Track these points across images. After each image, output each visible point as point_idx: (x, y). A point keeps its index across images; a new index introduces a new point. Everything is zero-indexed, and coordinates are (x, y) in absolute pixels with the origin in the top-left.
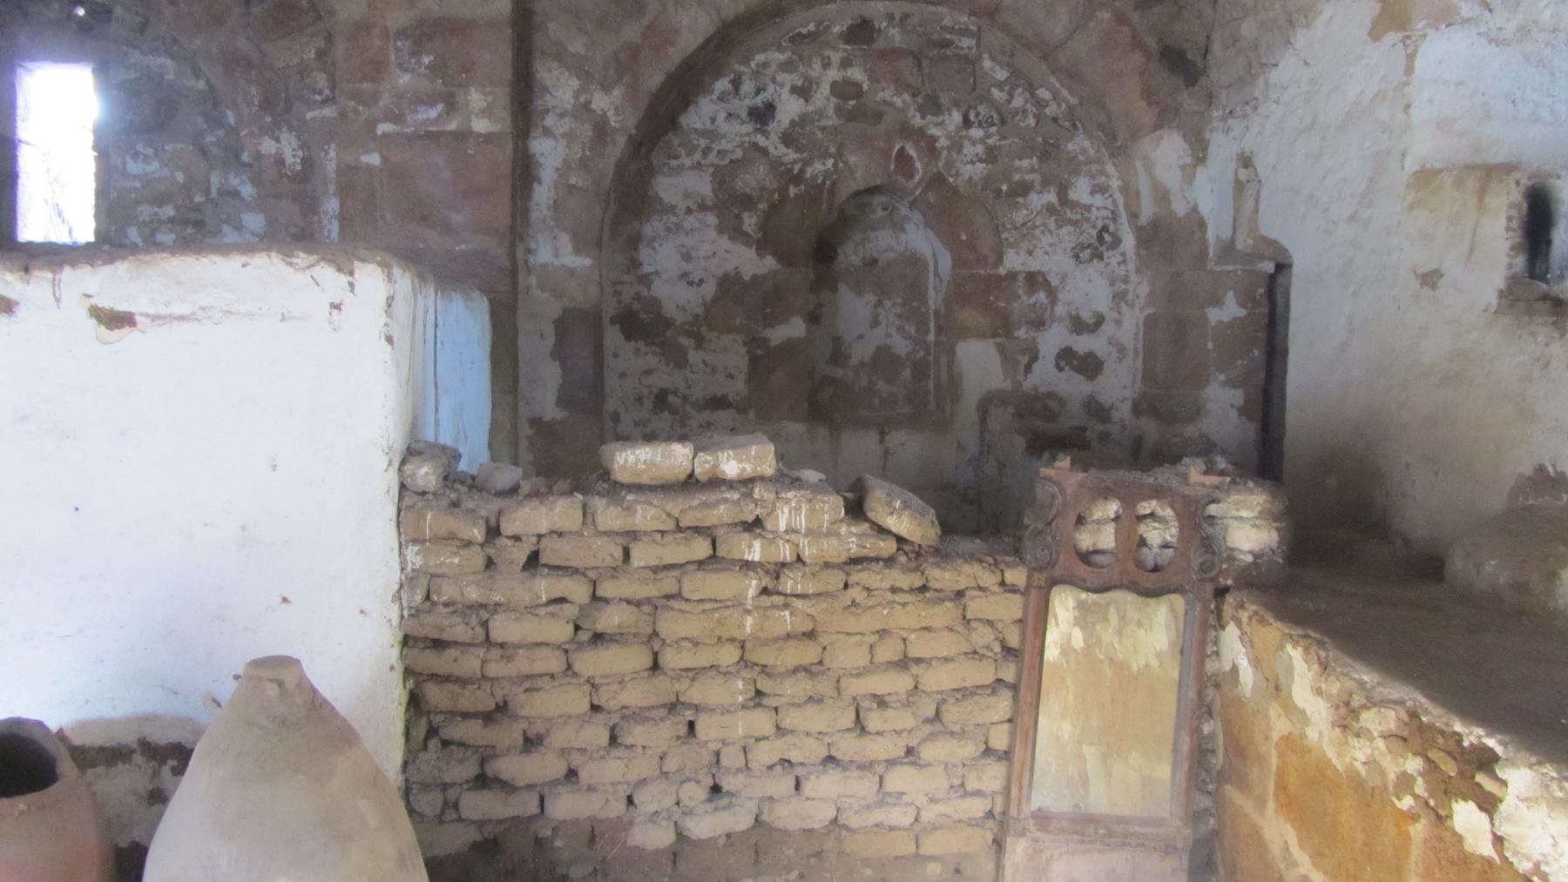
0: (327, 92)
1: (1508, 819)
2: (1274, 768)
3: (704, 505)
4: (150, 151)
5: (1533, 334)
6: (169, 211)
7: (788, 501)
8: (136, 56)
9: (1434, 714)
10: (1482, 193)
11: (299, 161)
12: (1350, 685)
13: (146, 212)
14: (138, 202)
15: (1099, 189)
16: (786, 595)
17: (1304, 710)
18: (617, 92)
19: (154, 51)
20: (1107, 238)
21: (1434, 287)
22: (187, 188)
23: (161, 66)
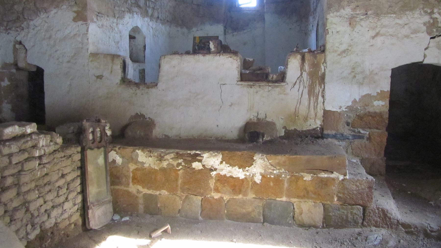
1: (205, 162)
2: (131, 176)
3: (24, 143)
7: (41, 138)
9: (181, 152)
10: (113, 60)
12: (159, 153)
16: (43, 164)
17: (143, 162)
21: (101, 79)
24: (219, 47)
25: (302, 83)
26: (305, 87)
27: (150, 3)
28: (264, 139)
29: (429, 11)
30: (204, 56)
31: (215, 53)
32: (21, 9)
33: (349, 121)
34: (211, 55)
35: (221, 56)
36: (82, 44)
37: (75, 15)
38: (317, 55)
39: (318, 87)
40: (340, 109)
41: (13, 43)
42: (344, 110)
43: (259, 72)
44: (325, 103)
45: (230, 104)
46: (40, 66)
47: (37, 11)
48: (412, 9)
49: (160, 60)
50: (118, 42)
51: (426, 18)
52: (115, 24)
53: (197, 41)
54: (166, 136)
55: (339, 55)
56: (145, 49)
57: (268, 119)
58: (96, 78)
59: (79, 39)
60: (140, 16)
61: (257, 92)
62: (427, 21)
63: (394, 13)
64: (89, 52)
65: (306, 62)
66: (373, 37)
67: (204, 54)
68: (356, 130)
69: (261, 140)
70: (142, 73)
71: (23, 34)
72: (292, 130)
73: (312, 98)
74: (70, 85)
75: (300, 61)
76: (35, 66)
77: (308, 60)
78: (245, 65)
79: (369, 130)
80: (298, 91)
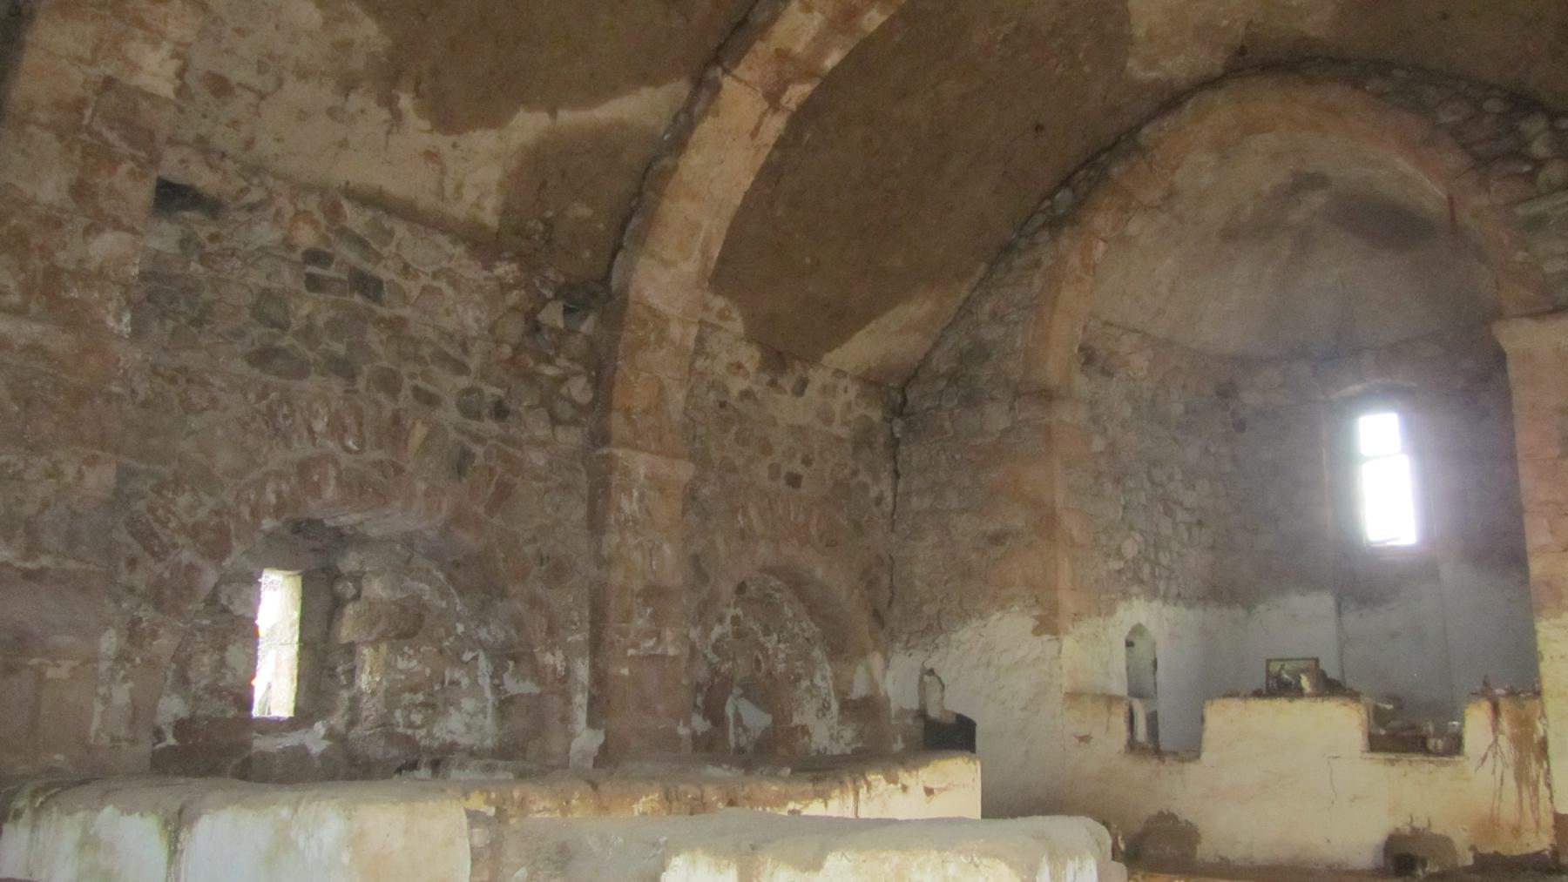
0: (578, 624)
4: (411, 652)
6: (420, 697)
8: (408, 582)
10: (1109, 708)
11: (563, 669)
13: (407, 697)
14: (402, 691)
18: (699, 628)
19: (420, 579)
20: (826, 705)
22: (430, 679)
23: (421, 590)
25: (1498, 757)
26: (1506, 765)
28: (1427, 869)
31: (1312, 696)
34: (1305, 699)
35: (1325, 702)
37: (1038, 623)
38: (1525, 703)
39: (1534, 766)
43: (1405, 734)
44: (1555, 800)
47: (964, 616)
49: (1202, 708)
50: (1107, 663)
52: (1100, 630)
54: (1222, 858)
57: (1436, 830)
58: (1077, 741)
60: (1142, 601)
61: (1405, 775)
64: (1064, 692)
65: (1503, 714)
69: (1420, 872)
70: (1152, 720)
72: (1489, 855)
73: (1524, 788)
75: (1490, 713)
76: (954, 713)
78: (1378, 716)
80: (1494, 773)
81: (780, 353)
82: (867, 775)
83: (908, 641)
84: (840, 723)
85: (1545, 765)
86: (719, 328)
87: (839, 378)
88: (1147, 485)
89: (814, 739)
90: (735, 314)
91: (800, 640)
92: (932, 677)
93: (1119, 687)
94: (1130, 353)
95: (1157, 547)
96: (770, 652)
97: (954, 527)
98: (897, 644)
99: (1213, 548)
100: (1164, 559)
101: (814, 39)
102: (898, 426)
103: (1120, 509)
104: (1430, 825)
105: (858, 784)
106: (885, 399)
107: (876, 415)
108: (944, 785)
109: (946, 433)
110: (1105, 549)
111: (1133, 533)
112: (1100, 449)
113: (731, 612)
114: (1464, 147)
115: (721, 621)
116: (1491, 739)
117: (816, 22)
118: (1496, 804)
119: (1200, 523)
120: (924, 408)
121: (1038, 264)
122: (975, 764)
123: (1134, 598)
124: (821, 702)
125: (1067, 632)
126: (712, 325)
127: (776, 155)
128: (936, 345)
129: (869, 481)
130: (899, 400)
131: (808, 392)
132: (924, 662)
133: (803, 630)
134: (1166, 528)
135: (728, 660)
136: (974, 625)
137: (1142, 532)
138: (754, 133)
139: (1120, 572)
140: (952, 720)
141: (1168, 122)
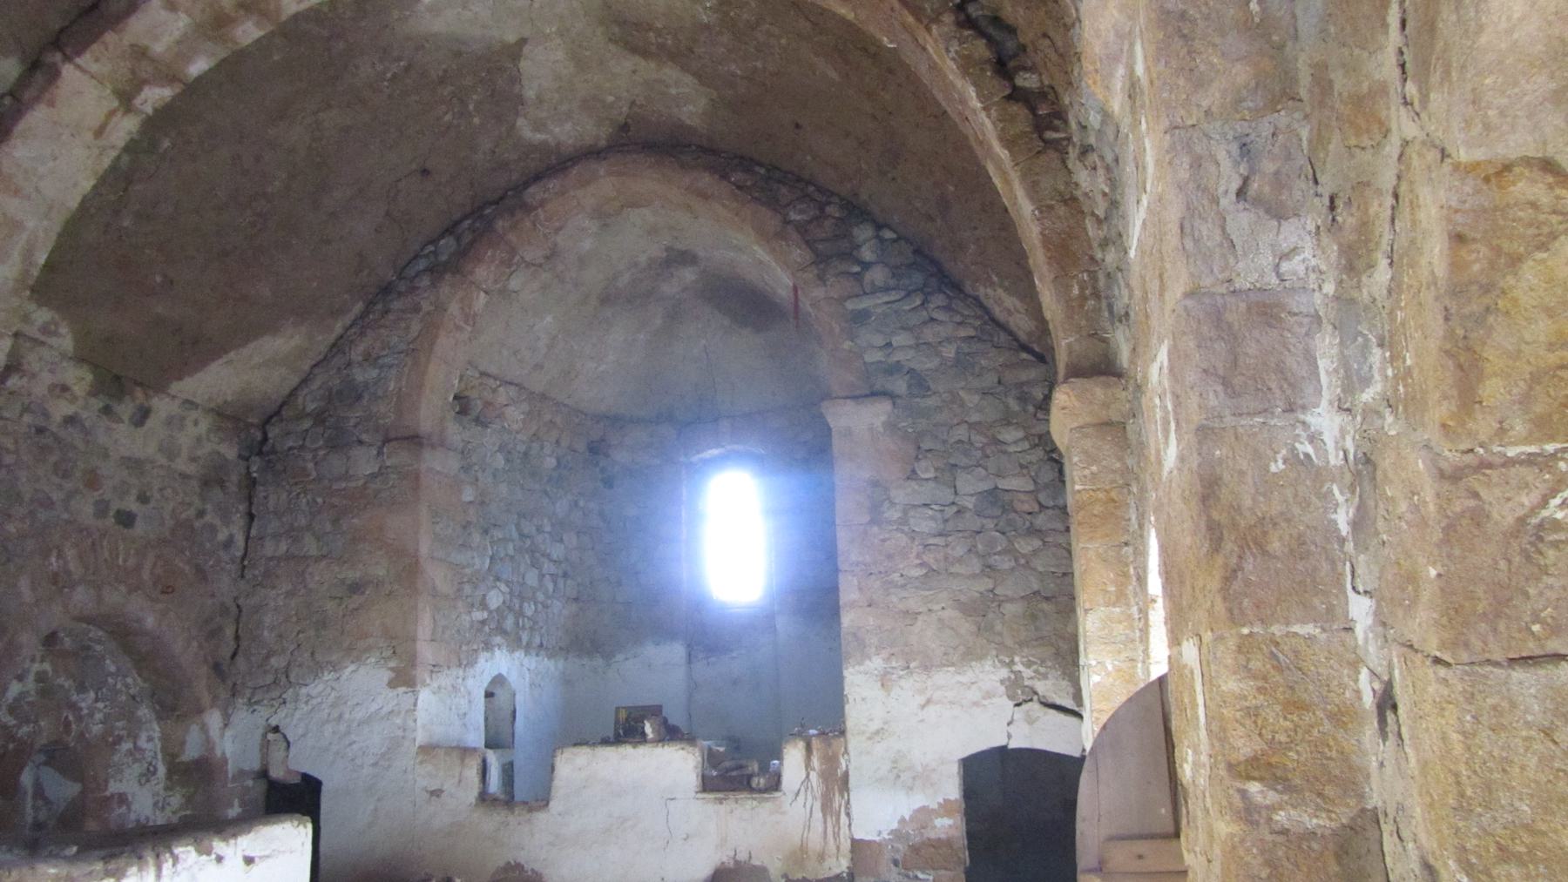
5: (498, 814)
10: (463, 760)
15: (150, 739)
20: (151, 769)
21: (438, 796)
24: (663, 730)
25: (809, 793)
26: (814, 798)
27: (526, 620)
29: (1007, 660)
30: (634, 747)
32: (284, 664)
33: (898, 857)
35: (666, 747)
36: (404, 730)
38: (832, 741)
39: (837, 797)
40: (879, 835)
41: (261, 731)
42: (887, 837)
43: (734, 773)
44: (853, 828)
45: (685, 836)
46: (311, 773)
47: (317, 669)
48: (981, 658)
50: (465, 714)
51: (1004, 673)
52: (460, 680)
53: (623, 715)
55: (870, 738)
56: (514, 717)
58: (428, 796)
59: (398, 721)
61: (732, 812)
62: (1006, 676)
63: (953, 665)
64: (417, 745)
65: (815, 753)
66: (923, 707)
67: (635, 744)
68: (911, 873)
70: (508, 772)
71: (282, 713)
73: (829, 819)
74: (376, 810)
75: (804, 752)
76: (298, 772)
77: (818, 749)
78: (711, 759)
79: (932, 872)
80: (805, 806)
81: (117, 378)
82: (173, 848)
83: (253, 694)
84: (167, 789)
85: (846, 797)
86: (43, 343)
87: (191, 409)
88: (515, 535)
89: (133, 807)
90: (64, 330)
91: (124, 698)
92: (277, 735)
93: (476, 738)
94: (506, 405)
95: (522, 598)
96: (85, 711)
97: (310, 574)
98: (240, 701)
99: (576, 600)
100: (529, 610)
101: (178, 42)
102: (256, 465)
103: (488, 561)
104: (750, 857)
105: (162, 857)
106: (243, 435)
107: (230, 452)
108: (267, 853)
109: (309, 475)
110: (469, 600)
111: (498, 584)
112: (470, 498)
113: (36, 667)
114: (807, 242)
115: (20, 678)
116: (804, 776)
117: (181, 24)
118: (805, 836)
119: (565, 575)
120: (286, 448)
121: (416, 309)
122: (305, 827)
123: (496, 649)
124: (146, 765)
125: (424, 684)
126: (35, 341)
127: (126, 158)
128: (305, 381)
129: (217, 522)
130: (259, 436)
131: (150, 423)
132: (267, 720)
133: (127, 686)
134: (532, 578)
135: (28, 722)
136: (326, 678)
137: (507, 583)
138: (99, 132)
139: (483, 622)
140: (297, 780)
141: (553, 184)
